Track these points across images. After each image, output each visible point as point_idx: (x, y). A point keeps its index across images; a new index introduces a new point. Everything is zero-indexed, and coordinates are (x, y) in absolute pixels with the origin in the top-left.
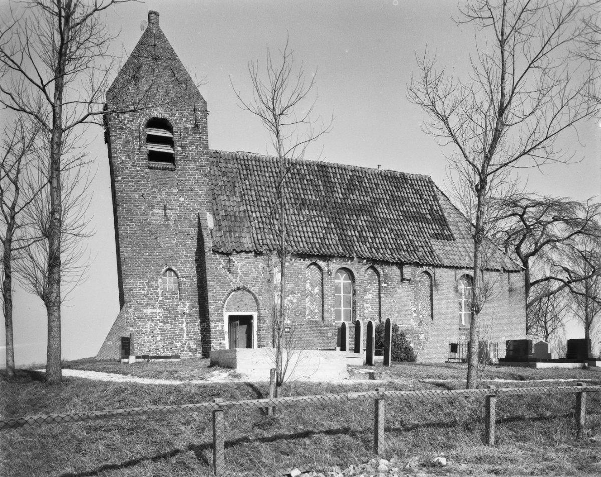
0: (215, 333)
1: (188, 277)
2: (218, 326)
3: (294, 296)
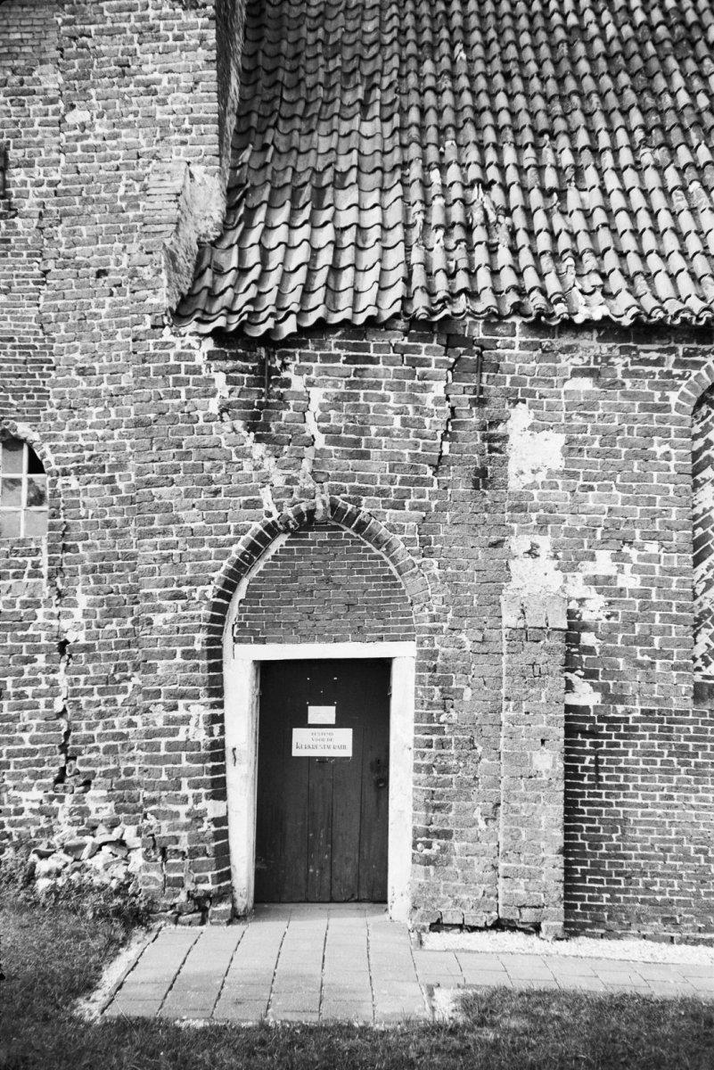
0: (165, 760)
1: (89, 470)
2: (186, 720)
3: (626, 559)
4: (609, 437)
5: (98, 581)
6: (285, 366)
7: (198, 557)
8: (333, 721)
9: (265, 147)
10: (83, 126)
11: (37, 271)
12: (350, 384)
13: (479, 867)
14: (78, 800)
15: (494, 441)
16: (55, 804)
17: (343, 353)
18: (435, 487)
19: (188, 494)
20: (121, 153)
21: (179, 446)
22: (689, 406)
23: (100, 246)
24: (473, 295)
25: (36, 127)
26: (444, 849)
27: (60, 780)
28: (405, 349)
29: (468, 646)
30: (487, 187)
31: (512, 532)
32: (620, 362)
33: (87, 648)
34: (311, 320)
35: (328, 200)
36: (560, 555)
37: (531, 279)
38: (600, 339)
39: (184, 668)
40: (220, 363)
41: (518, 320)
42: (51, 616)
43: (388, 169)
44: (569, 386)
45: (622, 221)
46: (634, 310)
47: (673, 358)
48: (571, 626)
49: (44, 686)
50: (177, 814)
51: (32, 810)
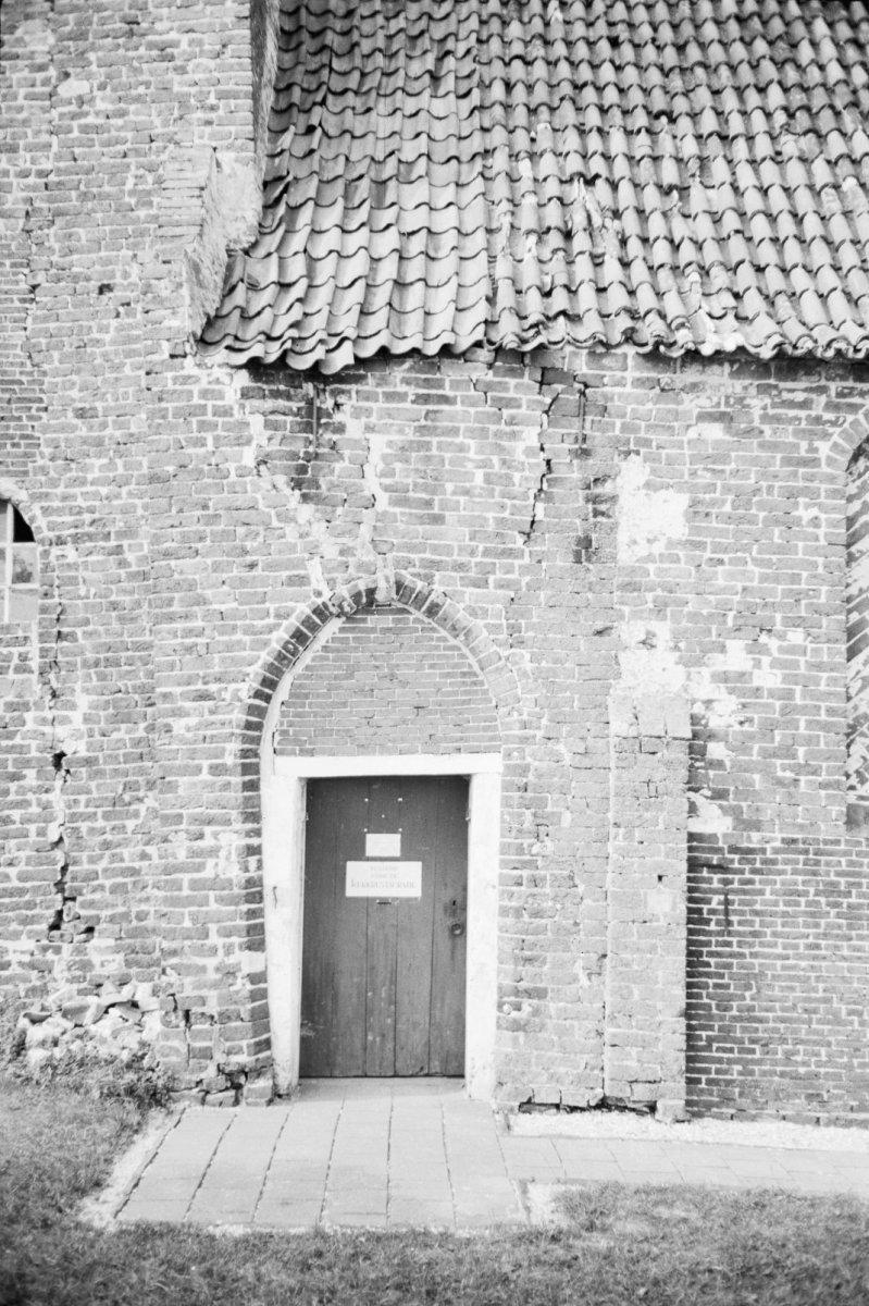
0: (189, 901)
1: (90, 537)
2: (213, 852)
3: (765, 650)
4: (743, 498)
5: (102, 677)
6: (337, 406)
7: (229, 647)
8: (397, 854)
9: (310, 130)
10: (81, 101)
11: (24, 286)
12: (421, 429)
13: (580, 1032)
14: (79, 951)
15: (599, 504)
16: (50, 956)
17: (412, 391)
18: (527, 560)
19: (216, 568)
20: (129, 135)
21: (205, 507)
22: (844, 460)
23: (103, 254)
24: (573, 318)
25: (21, 101)
26: (536, 1012)
27: (55, 926)
28: (488, 387)
29: (568, 759)
30: (590, 182)
31: (622, 617)
32: (757, 404)
33: (88, 762)
34: (369, 349)
35: (390, 197)
36: (682, 645)
37: (645, 299)
38: (733, 375)
39: (210, 786)
40: (257, 403)
41: (630, 350)
42: (44, 721)
43: (465, 158)
44: (692, 434)
45: (760, 227)
46: (777, 339)
47: (823, 399)
48: (695, 736)
49: (35, 810)
50: (203, 969)
51: (21, 964)
